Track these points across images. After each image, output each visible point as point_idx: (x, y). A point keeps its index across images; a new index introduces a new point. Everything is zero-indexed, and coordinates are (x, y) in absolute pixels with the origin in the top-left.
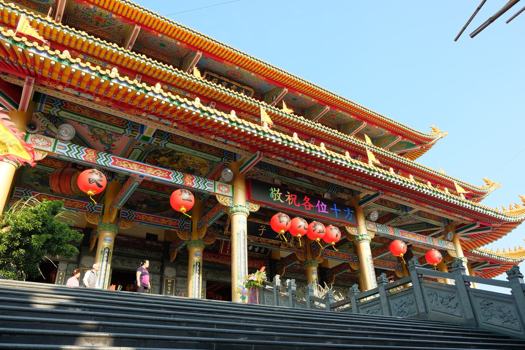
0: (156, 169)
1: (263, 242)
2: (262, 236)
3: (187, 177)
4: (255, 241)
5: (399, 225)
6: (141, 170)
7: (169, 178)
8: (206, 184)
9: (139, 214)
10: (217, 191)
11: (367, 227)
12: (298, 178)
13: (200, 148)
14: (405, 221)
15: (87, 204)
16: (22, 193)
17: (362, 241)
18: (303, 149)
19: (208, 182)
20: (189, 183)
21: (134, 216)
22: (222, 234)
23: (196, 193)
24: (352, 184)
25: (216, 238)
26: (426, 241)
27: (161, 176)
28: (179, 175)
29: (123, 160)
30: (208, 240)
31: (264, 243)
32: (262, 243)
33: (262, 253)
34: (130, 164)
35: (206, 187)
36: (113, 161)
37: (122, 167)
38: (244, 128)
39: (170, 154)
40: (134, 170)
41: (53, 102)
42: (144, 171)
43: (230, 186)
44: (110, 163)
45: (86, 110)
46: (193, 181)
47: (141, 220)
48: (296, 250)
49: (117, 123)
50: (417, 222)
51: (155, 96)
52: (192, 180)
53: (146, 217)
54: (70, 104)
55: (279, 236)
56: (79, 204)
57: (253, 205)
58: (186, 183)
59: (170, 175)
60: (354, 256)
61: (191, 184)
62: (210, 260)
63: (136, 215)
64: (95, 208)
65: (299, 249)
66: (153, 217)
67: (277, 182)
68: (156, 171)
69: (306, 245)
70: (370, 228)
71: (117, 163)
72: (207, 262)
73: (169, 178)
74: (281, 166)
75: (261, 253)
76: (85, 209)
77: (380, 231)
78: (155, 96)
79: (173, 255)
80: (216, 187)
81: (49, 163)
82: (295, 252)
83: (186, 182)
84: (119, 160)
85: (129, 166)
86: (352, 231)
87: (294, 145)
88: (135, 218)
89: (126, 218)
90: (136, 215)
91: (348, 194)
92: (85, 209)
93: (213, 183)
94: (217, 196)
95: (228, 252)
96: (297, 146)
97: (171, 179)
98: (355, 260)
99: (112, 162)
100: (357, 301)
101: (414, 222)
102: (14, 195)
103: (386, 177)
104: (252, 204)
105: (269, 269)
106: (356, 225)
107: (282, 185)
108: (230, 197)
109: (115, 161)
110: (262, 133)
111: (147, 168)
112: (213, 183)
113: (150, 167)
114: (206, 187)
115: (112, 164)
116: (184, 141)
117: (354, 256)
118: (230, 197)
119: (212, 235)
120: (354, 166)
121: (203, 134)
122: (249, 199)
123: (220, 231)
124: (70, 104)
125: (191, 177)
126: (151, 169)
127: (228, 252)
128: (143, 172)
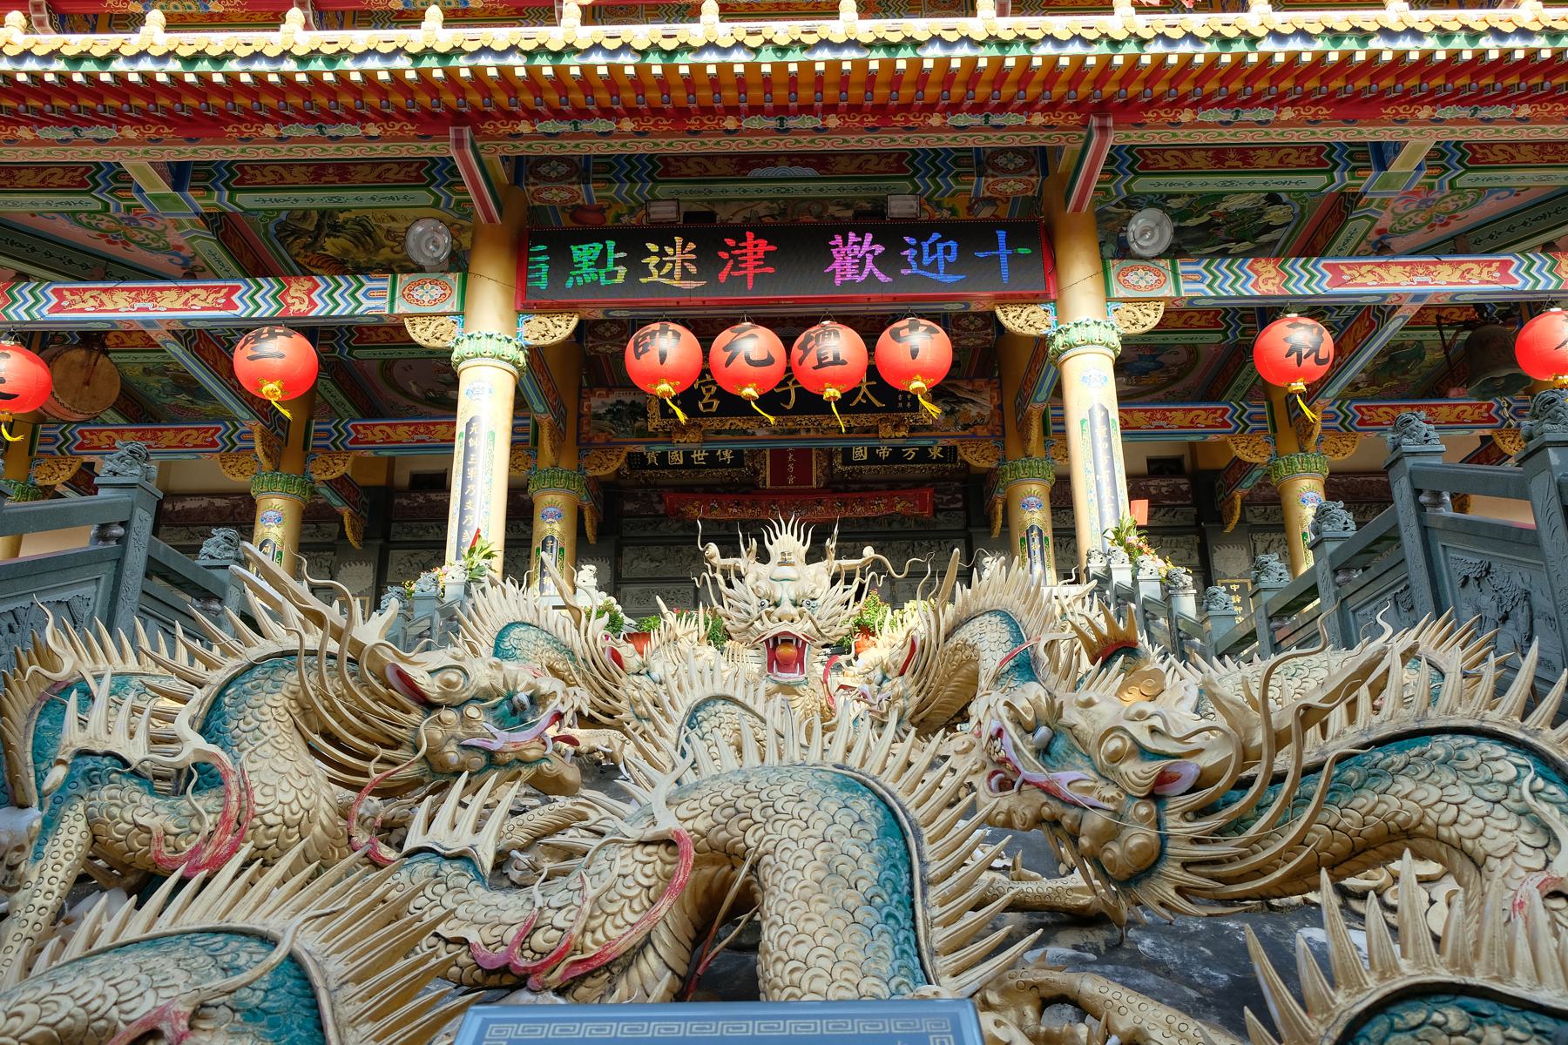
0: (187, 289)
1: (808, 430)
2: (795, 411)
3: (294, 286)
4: (775, 432)
5: (1441, 233)
6: (141, 305)
7: (229, 305)
8: (359, 295)
9: (365, 427)
10: (402, 307)
11: (1114, 284)
12: (757, 172)
13: (343, 179)
14: (138, 244)
15: (218, 430)
16: (55, 437)
17: (1069, 353)
18: (628, 62)
19: (368, 285)
20: (298, 307)
21: (349, 434)
22: (642, 432)
23: (313, 332)
24: (268, 141)
25: (629, 448)
26: (1506, 278)
27: (203, 309)
28: (345, 285)
29: (85, 290)
30: (597, 461)
31: (812, 434)
32: (803, 434)
33: (934, 462)
34: (104, 297)
35: (360, 304)
36: (55, 300)
37: (82, 310)
38: (244, 67)
39: (328, 222)
40: (116, 310)
41: (210, 175)
42: (149, 305)
43: (454, 279)
44: (45, 311)
45: (296, 170)
46: (314, 296)
47: (373, 442)
48: (953, 432)
49: (401, 176)
50: (1525, 198)
51: (18, 67)
52: (310, 292)
53: (388, 429)
54: (252, 167)
55: (865, 396)
56: (195, 433)
57: (547, 321)
58: (287, 310)
59: (235, 298)
60: (1250, 410)
61: (304, 307)
62: (725, 517)
63: (357, 432)
64: (239, 437)
65: (965, 427)
66: (410, 425)
67: (664, 211)
68: (188, 295)
69: (1000, 407)
70: (1135, 287)
71: (65, 303)
72: (719, 523)
73: (313, 304)
74: (670, 151)
75: (931, 461)
76: (214, 444)
77: (1188, 289)
78: (18, 67)
79: (353, 530)
80: (398, 294)
81: (384, 336)
82: (953, 442)
83: (289, 305)
84: (73, 292)
85: (102, 304)
86: (1020, 320)
87: (471, 63)
88: (355, 441)
89: (327, 447)
90: (357, 432)
91: (1018, 171)
92: (214, 444)
93: (387, 285)
94: (406, 321)
95: (791, 481)
96: (596, 59)
97: (236, 307)
98: (1253, 426)
99: (51, 304)
100: (1340, 578)
101: (1513, 202)
102: (38, 448)
103: (994, 52)
104: (543, 319)
105: (962, 513)
106: (1047, 292)
107: (689, 216)
108: (454, 314)
109: (61, 297)
110: (320, 63)
111: (158, 294)
112: (387, 285)
113: (169, 289)
114: (360, 304)
115: (51, 311)
116: (709, 166)
117: (1250, 410)
118: (454, 314)
119: (608, 442)
120: (794, 60)
121: (693, 124)
122: (527, 303)
123: (637, 424)
124: (252, 167)
125: (308, 285)
126: (173, 294)
127: (791, 481)
128: (147, 310)
